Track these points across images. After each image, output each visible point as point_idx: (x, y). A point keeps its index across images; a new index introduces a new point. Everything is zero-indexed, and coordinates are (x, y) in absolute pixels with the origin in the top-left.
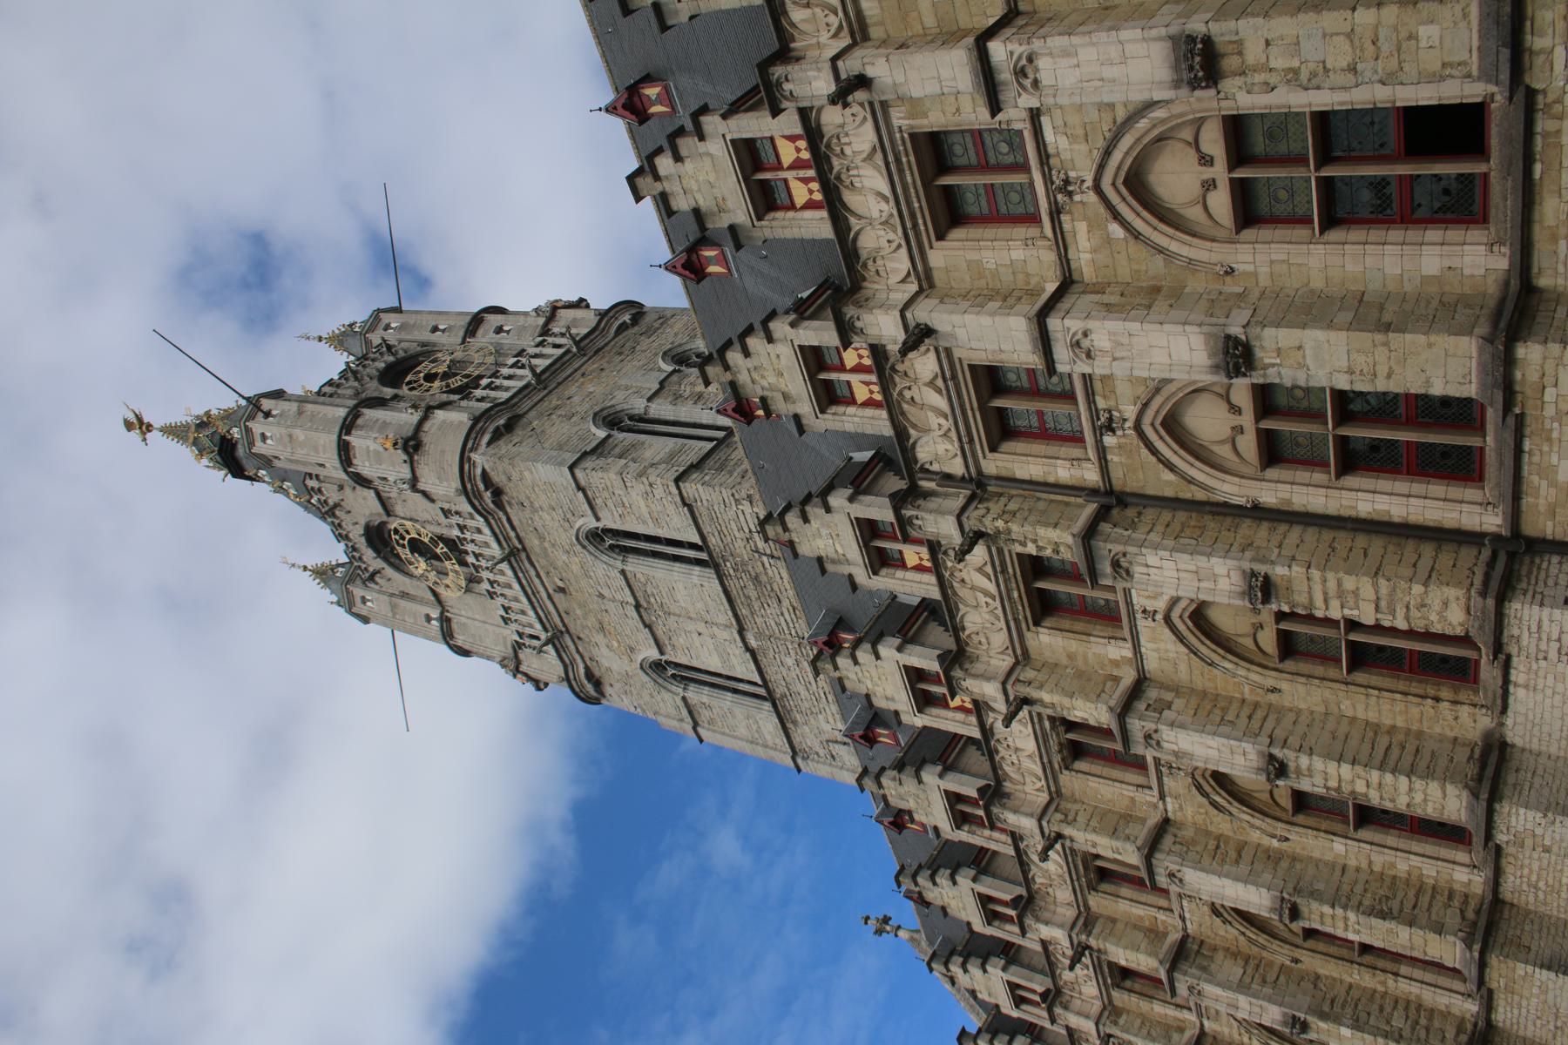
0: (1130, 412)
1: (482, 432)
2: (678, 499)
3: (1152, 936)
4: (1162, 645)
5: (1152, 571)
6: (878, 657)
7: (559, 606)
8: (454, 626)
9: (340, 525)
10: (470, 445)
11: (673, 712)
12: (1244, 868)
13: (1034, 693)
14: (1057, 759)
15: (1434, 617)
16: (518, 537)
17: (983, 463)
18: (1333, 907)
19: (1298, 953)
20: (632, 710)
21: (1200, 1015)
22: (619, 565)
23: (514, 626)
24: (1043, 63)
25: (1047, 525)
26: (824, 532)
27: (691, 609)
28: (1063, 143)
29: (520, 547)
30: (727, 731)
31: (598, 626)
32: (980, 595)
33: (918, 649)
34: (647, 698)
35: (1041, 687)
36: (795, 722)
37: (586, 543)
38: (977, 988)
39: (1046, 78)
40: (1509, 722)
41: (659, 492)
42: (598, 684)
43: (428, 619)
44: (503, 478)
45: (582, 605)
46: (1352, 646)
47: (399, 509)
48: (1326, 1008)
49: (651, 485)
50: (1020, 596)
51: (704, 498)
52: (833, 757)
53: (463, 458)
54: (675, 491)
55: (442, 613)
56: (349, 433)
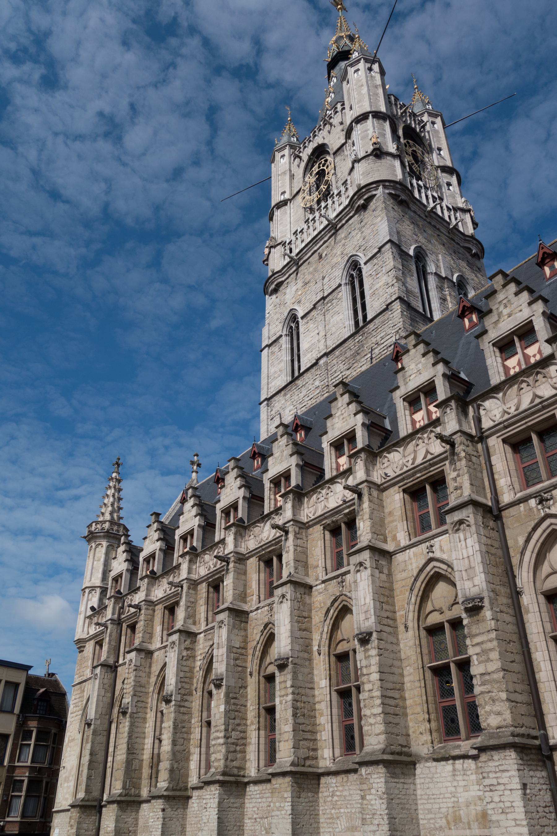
1: (394, 188)
2: (389, 301)
3: (243, 596)
4: (413, 561)
5: (463, 543)
6: (355, 414)
7: (311, 258)
8: (283, 208)
10: (387, 184)
11: (272, 332)
12: (298, 634)
13: (366, 498)
14: (328, 521)
15: (488, 708)
17: (494, 437)
18: (292, 686)
19: (255, 674)
20: (267, 312)
21: (205, 631)
22: (343, 282)
23: (293, 238)
25: (471, 480)
26: (420, 366)
27: (330, 326)
29: (338, 227)
30: (270, 362)
31: (307, 281)
32: (412, 456)
33: (366, 434)
35: (370, 501)
36: (285, 395)
37: (350, 261)
38: (185, 515)
40: (429, 764)
41: (391, 290)
42: (275, 291)
43: (283, 193)
45: (316, 270)
46: (446, 667)
47: (338, 159)
48: (231, 695)
49: (393, 285)
50: (418, 478)
51: (394, 314)
53: (378, 182)
54: (393, 299)
55: (289, 200)
56: (374, 117)
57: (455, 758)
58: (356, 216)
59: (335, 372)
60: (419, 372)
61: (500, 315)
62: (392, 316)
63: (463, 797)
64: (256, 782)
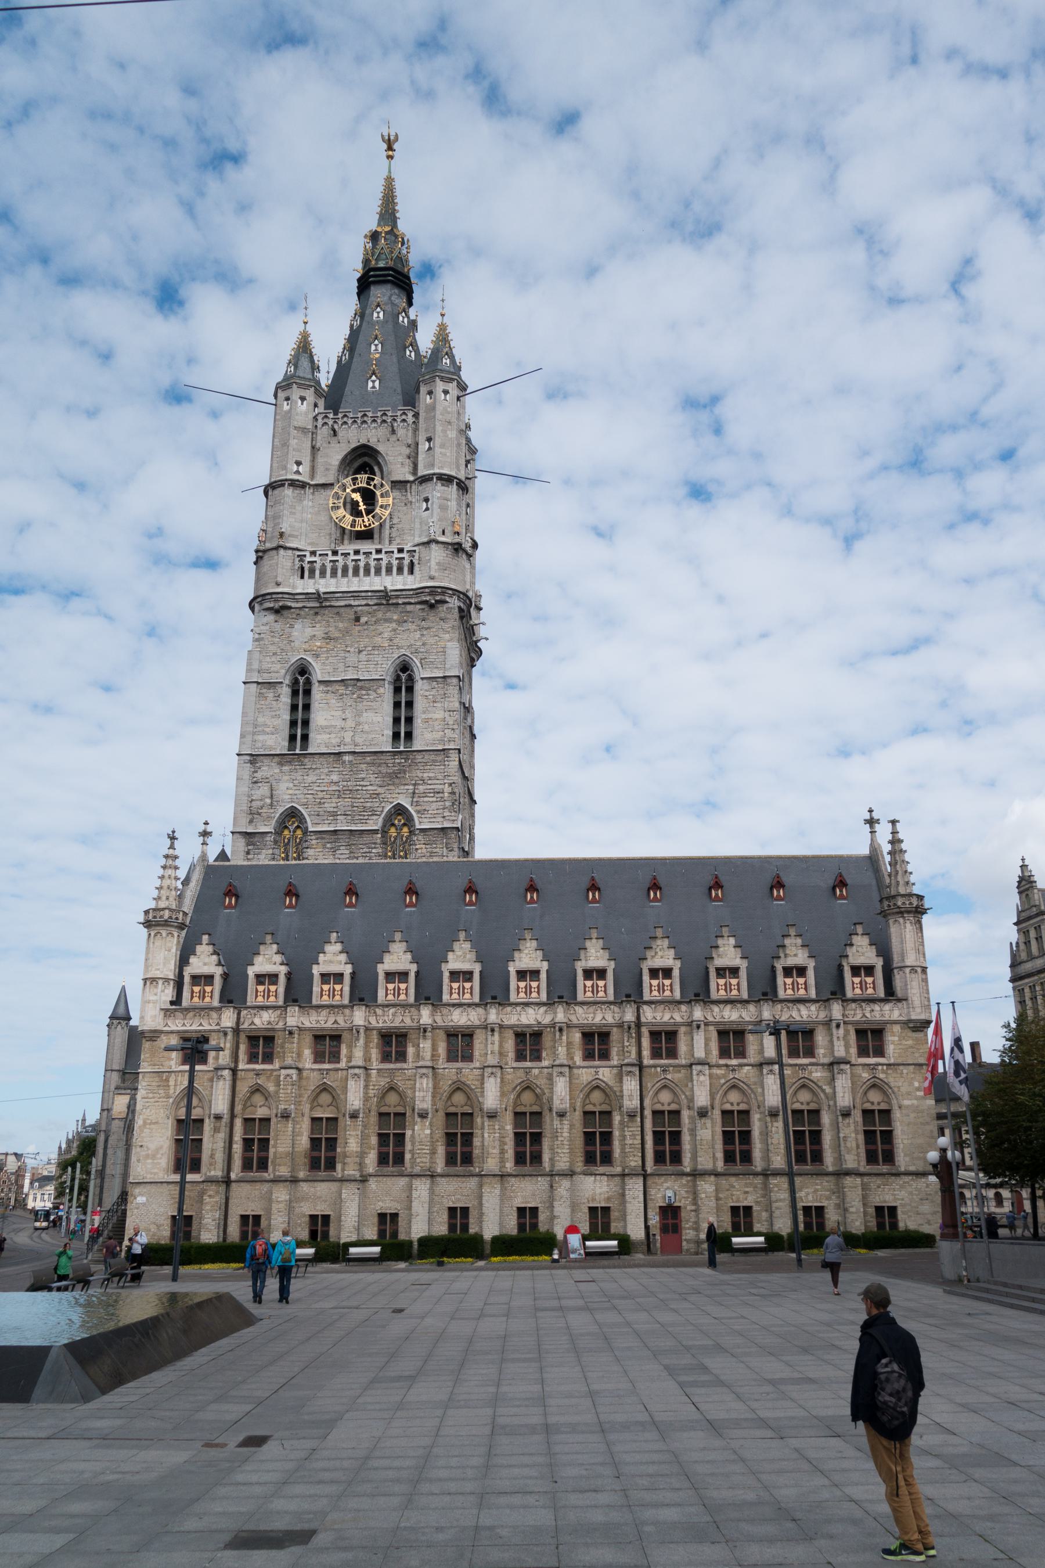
0: (669, 1077)
4: (584, 1075)
9: (374, 421)
10: (461, 596)
11: (265, 666)
14: (519, 1030)
16: (398, 604)
24: (773, 1076)
26: (598, 954)
28: (745, 1071)
29: (390, 602)
34: (272, 648)
37: (401, 659)
39: (769, 1076)
42: (277, 611)
44: (443, 615)
49: (453, 729)
51: (451, 763)
52: (256, 782)
55: (309, 484)
56: (457, 484)
57: (596, 1175)
58: (419, 607)
59: (363, 779)
60: (597, 958)
61: (656, 953)
62: (446, 763)
63: (598, 1191)
64: (442, 1176)
